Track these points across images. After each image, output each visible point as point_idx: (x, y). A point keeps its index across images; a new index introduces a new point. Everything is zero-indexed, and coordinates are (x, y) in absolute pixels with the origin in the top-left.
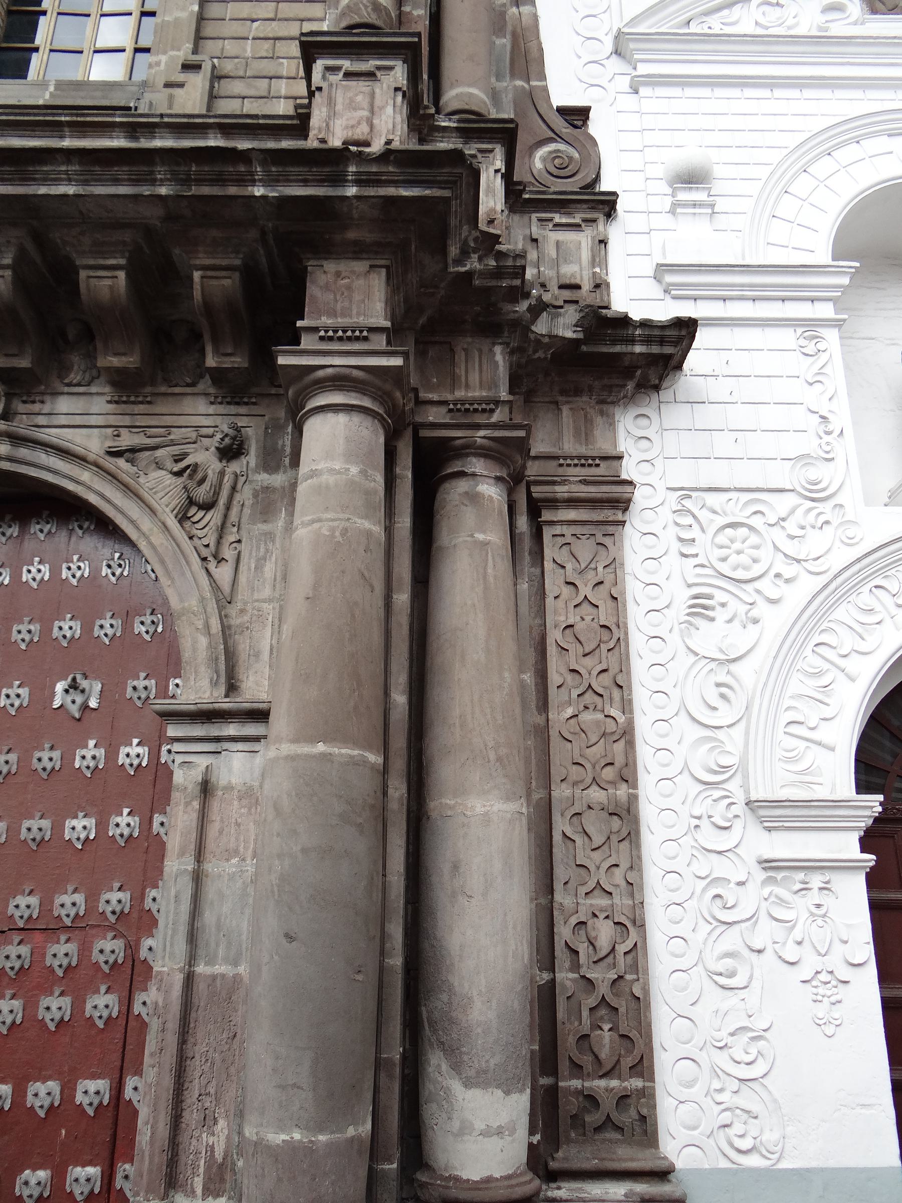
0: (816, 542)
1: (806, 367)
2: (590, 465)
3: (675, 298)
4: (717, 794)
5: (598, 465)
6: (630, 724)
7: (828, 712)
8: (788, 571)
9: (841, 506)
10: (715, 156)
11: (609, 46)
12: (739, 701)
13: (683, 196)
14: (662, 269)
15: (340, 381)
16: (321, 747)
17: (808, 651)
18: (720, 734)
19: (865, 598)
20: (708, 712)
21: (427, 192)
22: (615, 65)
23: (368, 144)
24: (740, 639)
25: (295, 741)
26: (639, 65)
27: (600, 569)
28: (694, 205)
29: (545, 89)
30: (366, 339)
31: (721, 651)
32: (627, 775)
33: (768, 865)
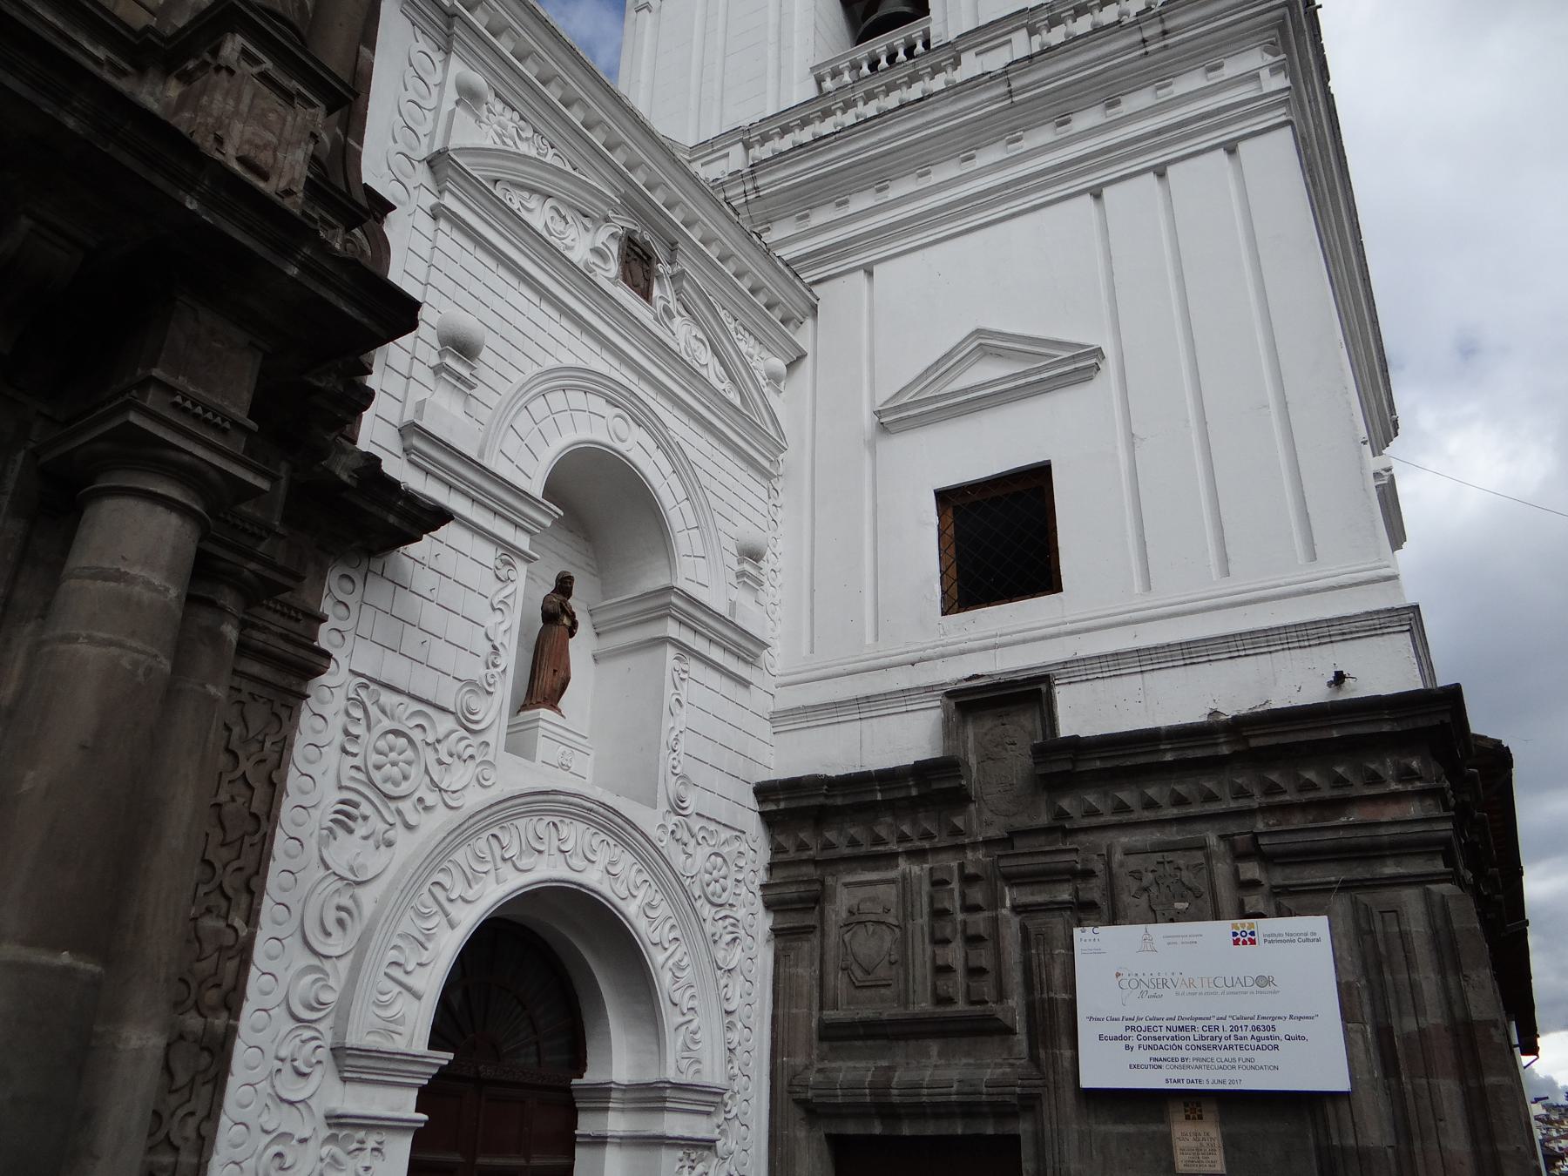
0: (460, 775)
1: (490, 586)
2: (290, 617)
3: (411, 461)
4: (307, 1034)
5: (298, 620)
6: (251, 938)
7: (425, 958)
8: (431, 798)
9: (487, 744)
10: (490, 340)
11: (424, 152)
12: (355, 930)
13: (449, 361)
14: (410, 430)
15: (189, 474)
16: (65, 958)
17: (425, 890)
18: (327, 965)
19: (481, 844)
20: (321, 937)
21: (365, 320)
22: (423, 175)
23: (265, 177)
24: (374, 861)
25: (26, 943)
26: (447, 194)
27: (268, 744)
28: (459, 378)
29: (359, 154)
30: (224, 431)
31: (352, 869)
32: (232, 1001)
33: (337, 1121)
